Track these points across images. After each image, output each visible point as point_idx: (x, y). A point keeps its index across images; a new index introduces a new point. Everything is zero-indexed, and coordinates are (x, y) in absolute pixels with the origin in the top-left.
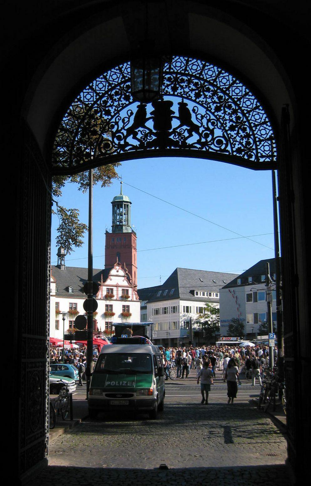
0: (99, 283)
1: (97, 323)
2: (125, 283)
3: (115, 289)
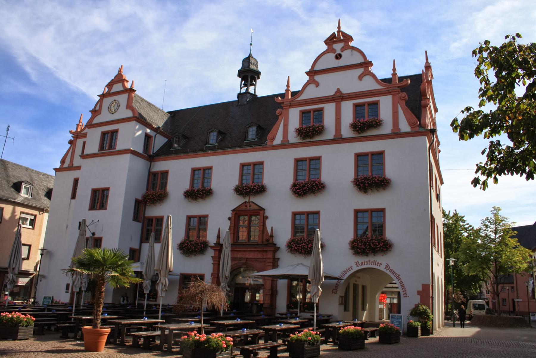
3: (329, 109)
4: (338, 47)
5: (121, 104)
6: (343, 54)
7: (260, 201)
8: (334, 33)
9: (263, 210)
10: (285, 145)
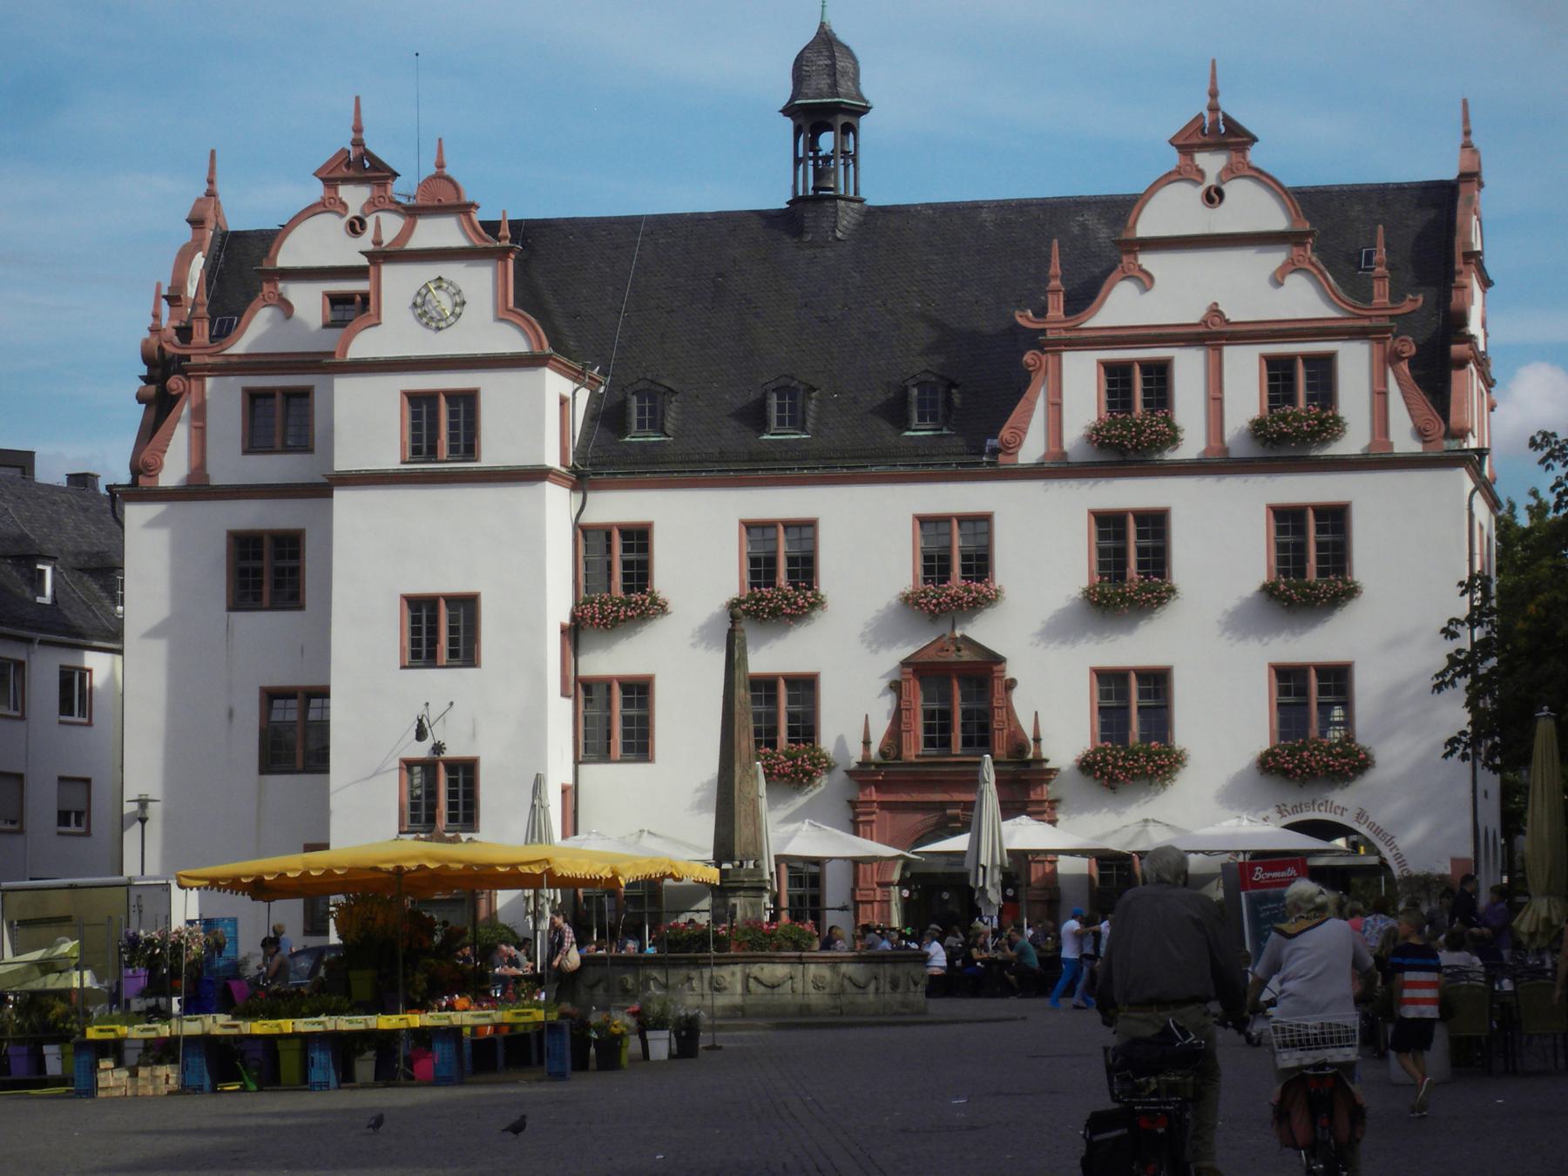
0: (1025, 319)
1: (1011, 684)
2: (1303, 299)
3: (1188, 367)
4: (1212, 163)
5: (466, 296)
6: (1225, 188)
7: (984, 631)
8: (1201, 116)
9: (998, 660)
10: (1056, 468)
